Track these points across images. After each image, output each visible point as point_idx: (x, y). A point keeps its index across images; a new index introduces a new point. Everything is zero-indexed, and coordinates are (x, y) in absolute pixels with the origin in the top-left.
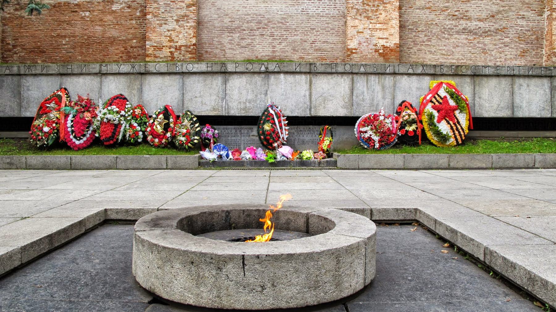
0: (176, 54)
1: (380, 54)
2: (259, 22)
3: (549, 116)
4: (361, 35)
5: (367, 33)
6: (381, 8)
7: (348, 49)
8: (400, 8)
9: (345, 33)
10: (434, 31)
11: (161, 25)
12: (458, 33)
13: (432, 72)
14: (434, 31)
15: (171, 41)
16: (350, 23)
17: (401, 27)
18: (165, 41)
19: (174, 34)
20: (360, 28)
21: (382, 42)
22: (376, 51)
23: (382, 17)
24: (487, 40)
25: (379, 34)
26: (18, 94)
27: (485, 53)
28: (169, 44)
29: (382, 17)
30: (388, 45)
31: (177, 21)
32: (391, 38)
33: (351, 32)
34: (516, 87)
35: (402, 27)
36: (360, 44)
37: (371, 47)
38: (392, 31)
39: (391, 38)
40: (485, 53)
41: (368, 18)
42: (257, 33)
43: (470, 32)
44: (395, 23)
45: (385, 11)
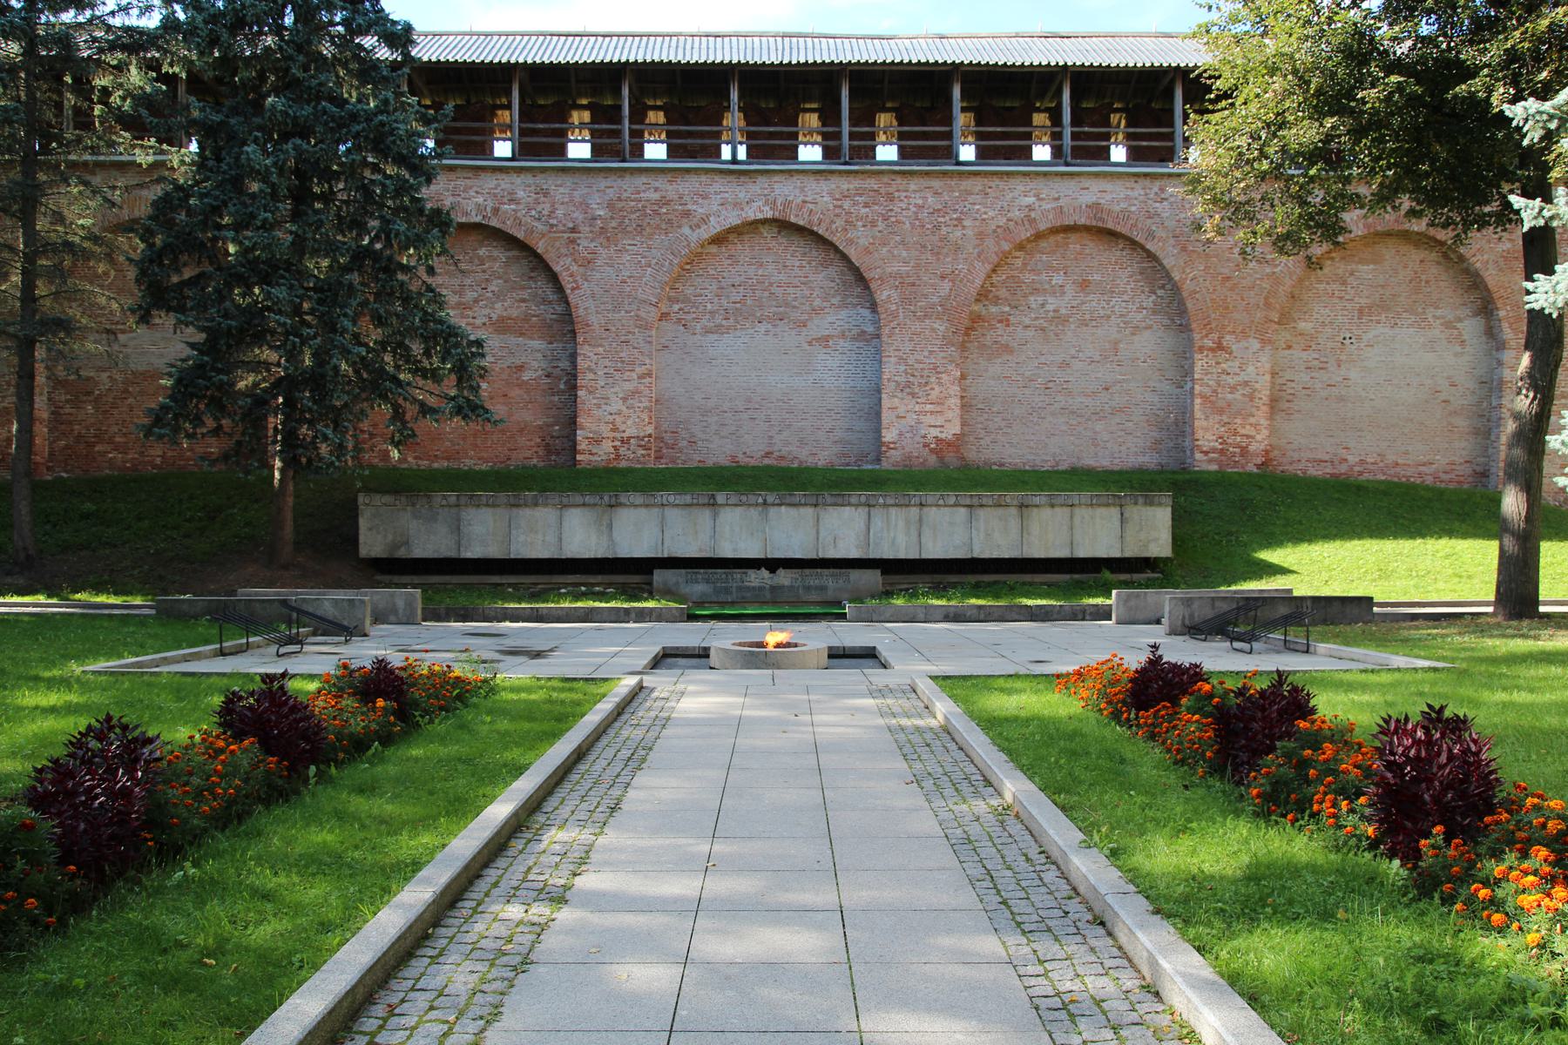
0: (622, 451)
1: (932, 451)
2: (749, 400)
3: (1118, 555)
4: (903, 421)
5: (911, 419)
6: (933, 379)
7: (883, 444)
8: (963, 377)
9: (878, 414)
10: (1016, 412)
11: (599, 406)
12: (1053, 414)
13: (968, 502)
14: (1016, 412)
15: (615, 430)
16: (886, 403)
17: (963, 406)
18: (605, 430)
19: (619, 419)
20: (901, 411)
21: (934, 432)
22: (926, 445)
23: (934, 394)
24: (1099, 427)
25: (930, 420)
26: (457, 528)
27: (1096, 446)
28: (611, 435)
29: (934, 394)
30: (943, 436)
31: (624, 399)
32: (947, 425)
33: (886, 416)
34: (1077, 520)
35: (966, 406)
36: (901, 434)
37: (918, 439)
38: (950, 415)
39: (947, 425)
40: (1096, 446)
41: (913, 395)
42: (745, 416)
43: (1073, 413)
44: (954, 402)
45: (940, 384)
